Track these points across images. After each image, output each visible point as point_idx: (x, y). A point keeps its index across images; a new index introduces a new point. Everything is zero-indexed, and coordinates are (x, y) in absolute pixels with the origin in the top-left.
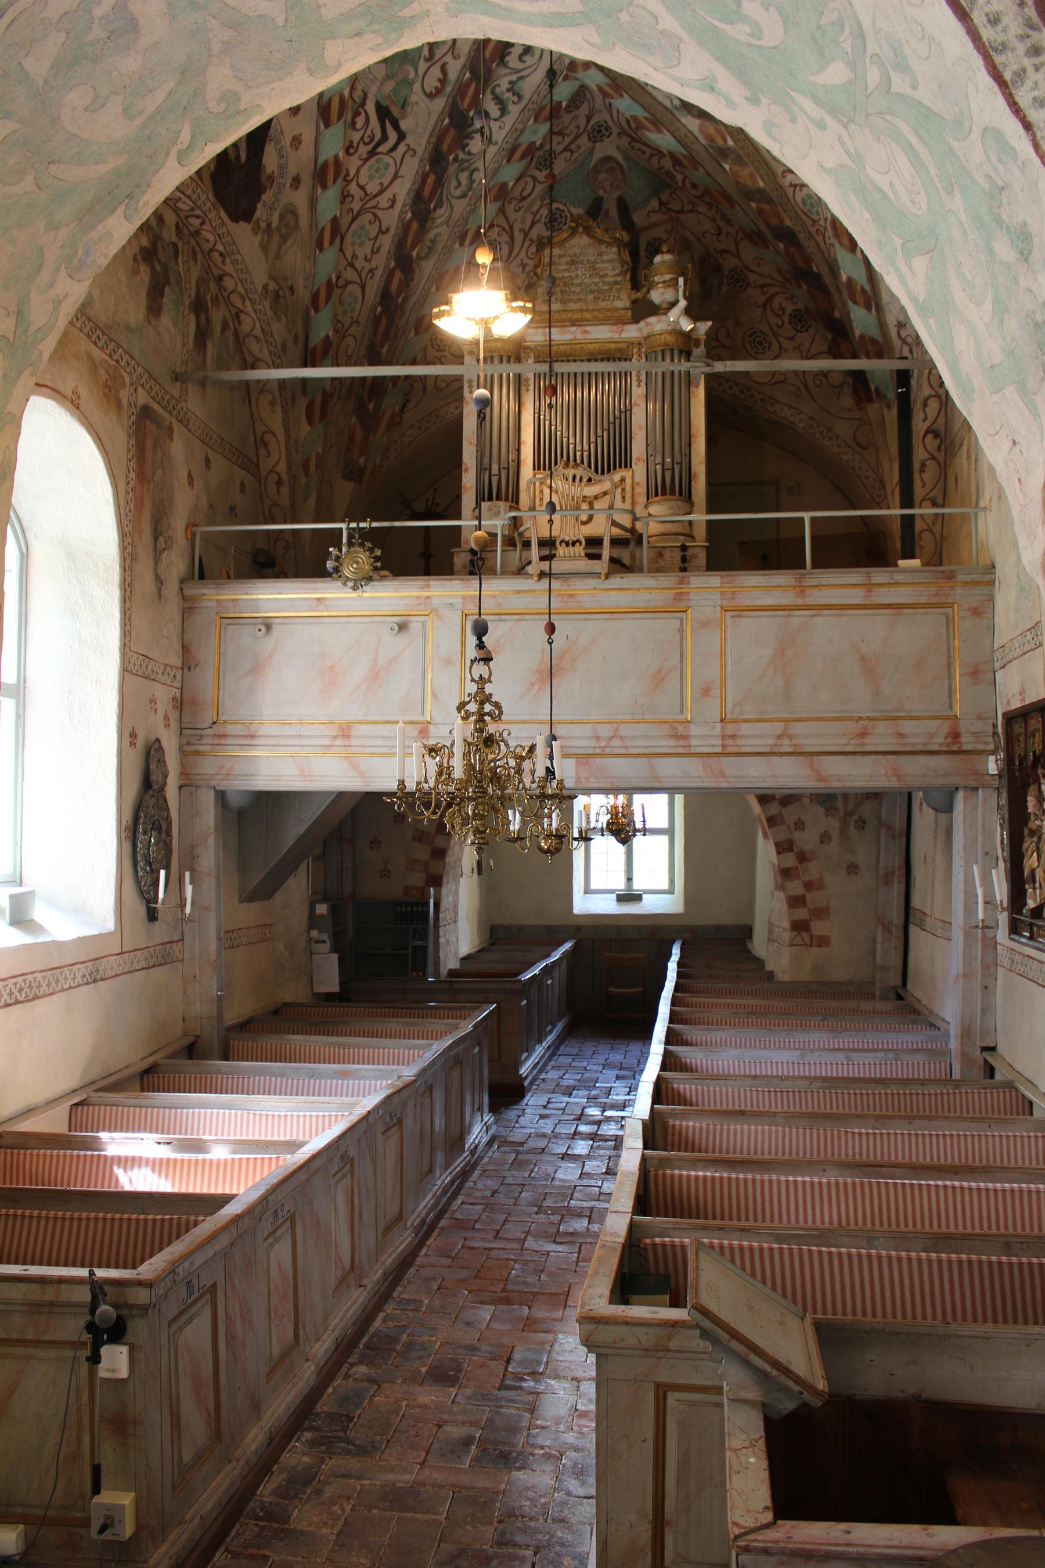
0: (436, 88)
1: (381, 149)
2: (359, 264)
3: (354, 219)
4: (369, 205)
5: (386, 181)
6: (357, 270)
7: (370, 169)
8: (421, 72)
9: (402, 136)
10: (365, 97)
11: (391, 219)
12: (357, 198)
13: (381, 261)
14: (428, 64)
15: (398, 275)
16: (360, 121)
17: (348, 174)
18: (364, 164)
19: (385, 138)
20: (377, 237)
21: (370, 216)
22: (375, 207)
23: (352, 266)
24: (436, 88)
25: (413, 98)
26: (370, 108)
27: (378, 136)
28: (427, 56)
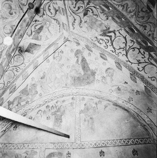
1: (113, 39)
2: (142, 60)
6: (144, 62)
8: (101, 20)
9: (114, 32)
10: (96, 38)
11: (136, 45)
15: (152, 53)
19: (110, 37)
20: (140, 52)
22: (130, 47)
23: (140, 63)
26: (100, 37)
27: (109, 38)
28: (96, 16)
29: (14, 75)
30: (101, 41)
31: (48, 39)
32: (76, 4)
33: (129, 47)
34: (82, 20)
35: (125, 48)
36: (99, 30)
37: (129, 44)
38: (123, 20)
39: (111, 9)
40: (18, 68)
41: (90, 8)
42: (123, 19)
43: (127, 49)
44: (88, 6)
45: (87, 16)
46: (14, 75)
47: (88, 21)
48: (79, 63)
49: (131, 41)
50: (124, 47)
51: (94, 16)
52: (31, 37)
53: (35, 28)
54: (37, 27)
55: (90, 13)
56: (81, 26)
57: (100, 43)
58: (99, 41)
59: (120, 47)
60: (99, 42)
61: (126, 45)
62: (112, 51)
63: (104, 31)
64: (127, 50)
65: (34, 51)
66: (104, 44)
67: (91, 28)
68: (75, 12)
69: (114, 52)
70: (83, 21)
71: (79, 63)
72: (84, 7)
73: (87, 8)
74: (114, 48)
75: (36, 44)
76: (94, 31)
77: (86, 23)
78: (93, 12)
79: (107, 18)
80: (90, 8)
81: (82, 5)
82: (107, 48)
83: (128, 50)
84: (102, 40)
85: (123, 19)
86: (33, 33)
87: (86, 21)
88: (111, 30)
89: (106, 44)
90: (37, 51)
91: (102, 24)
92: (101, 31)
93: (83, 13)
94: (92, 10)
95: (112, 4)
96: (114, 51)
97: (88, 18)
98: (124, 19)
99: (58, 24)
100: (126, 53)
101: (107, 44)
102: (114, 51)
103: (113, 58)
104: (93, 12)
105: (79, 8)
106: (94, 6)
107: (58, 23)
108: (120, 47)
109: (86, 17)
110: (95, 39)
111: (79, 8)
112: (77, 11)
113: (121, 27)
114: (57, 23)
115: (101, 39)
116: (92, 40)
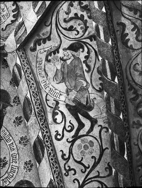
0: (101, 84)
1: (82, 133)
4: (91, 176)
7: (79, 146)
8: (89, 82)
9: (94, 122)
10: (57, 103)
12: (78, 170)
14: (90, 74)
16: (59, 118)
17: (63, 155)
18: (72, 145)
19: (81, 125)
22: (98, 176)
24: (101, 84)
25: (92, 96)
26: (62, 108)
27: (76, 125)
28: (87, 69)
30: (59, 118)
32: (71, 19)
33: (97, 174)
34: (61, 50)
35: (89, 169)
36: (73, 95)
38: (121, 117)
39: (116, 80)
41: (89, 47)
42: (121, 114)
43: (91, 176)
44: (88, 41)
45: (74, 53)
47: (69, 62)
49: (106, 166)
50: (87, 166)
51: (84, 65)
55: (82, 55)
56: (50, 58)
57: (55, 120)
58: (57, 114)
59: (82, 160)
60: (54, 114)
62: (63, 155)
63: (80, 104)
64: (89, 177)
66: (60, 128)
67: (63, 78)
68: (61, 28)
69: (65, 159)
70: (61, 54)
72: (77, 36)
73: (85, 43)
74: (71, 152)
76: (62, 87)
77: (62, 62)
79: (100, 88)
80: (89, 47)
81: (79, 29)
82: (59, 140)
83: (92, 180)
85: (121, 114)
87: (65, 58)
88: (92, 114)
89: (63, 132)
91: (85, 89)
92: (74, 101)
93: (72, 42)
94: (89, 52)
95: (125, 75)
96: (66, 157)
97: (73, 58)
98: (123, 116)
99: (14, 16)
100: (84, 181)
101: (65, 132)
102: (66, 157)
103: (55, 169)
104: (87, 57)
105: (71, 29)
106: (97, 50)
107: (15, 13)
108: (82, 160)
109: (69, 52)
110: (51, 103)
112: (65, 29)
113: (109, 123)
114: (13, 11)
115: (62, 113)
116: (46, 100)
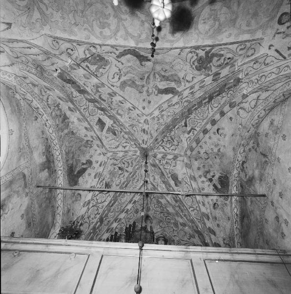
2: (90, 219)
3: (93, 206)
5: (103, 201)
11: (101, 211)
13: (95, 221)
15: (99, 223)
21: (96, 208)
26: (104, 182)
29: (81, 107)
31: (106, 138)
37: (100, 206)
40: (86, 110)
46: (81, 107)
48: (82, 166)
52: (110, 126)
53: (116, 130)
54: (116, 132)
55: (120, 172)
60: (101, 182)
61: (100, 203)
65: (98, 126)
70: (115, 167)
71: (82, 166)
75: (104, 128)
78: (121, 174)
84: (103, 185)
86: (113, 128)
90: (98, 128)
104: (121, 174)
105: (124, 163)
109: (118, 168)
111: (124, 163)
